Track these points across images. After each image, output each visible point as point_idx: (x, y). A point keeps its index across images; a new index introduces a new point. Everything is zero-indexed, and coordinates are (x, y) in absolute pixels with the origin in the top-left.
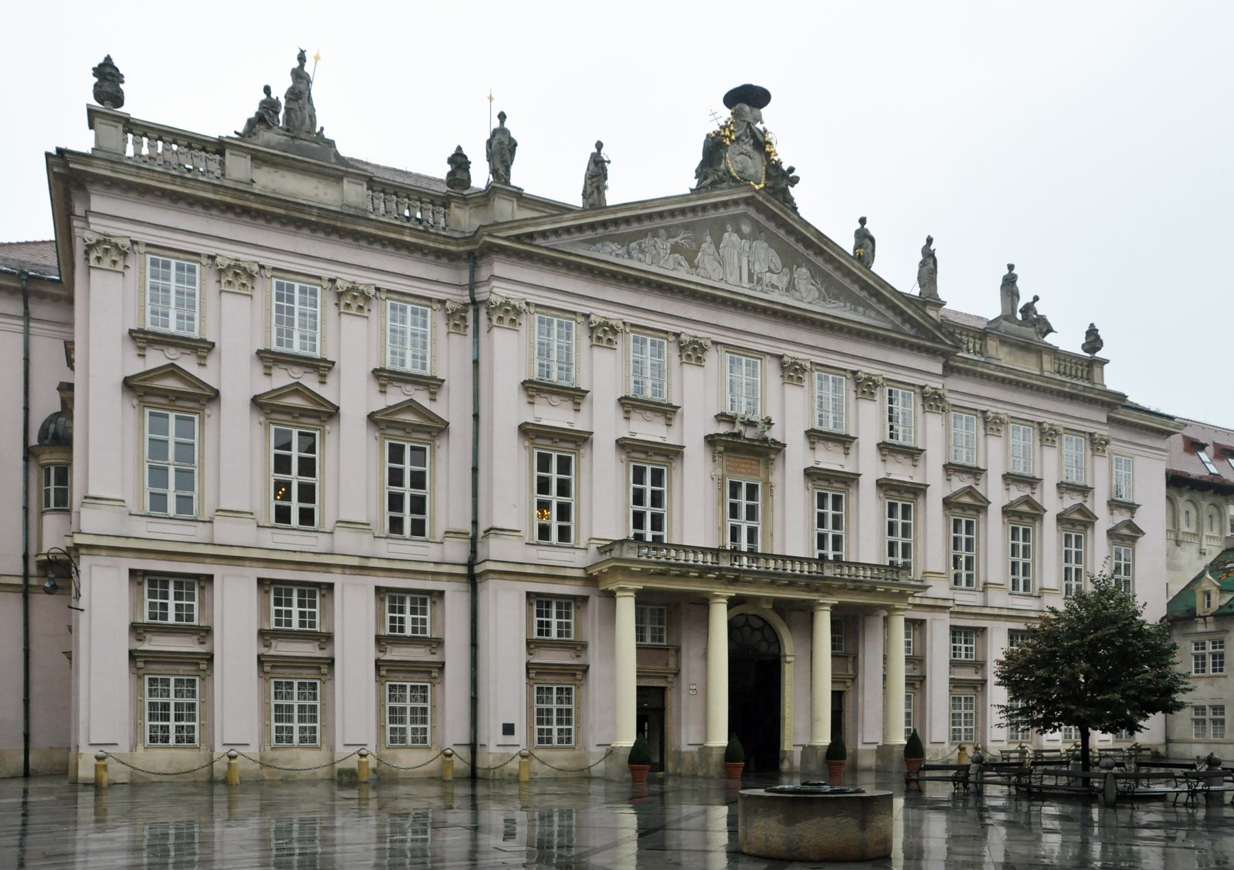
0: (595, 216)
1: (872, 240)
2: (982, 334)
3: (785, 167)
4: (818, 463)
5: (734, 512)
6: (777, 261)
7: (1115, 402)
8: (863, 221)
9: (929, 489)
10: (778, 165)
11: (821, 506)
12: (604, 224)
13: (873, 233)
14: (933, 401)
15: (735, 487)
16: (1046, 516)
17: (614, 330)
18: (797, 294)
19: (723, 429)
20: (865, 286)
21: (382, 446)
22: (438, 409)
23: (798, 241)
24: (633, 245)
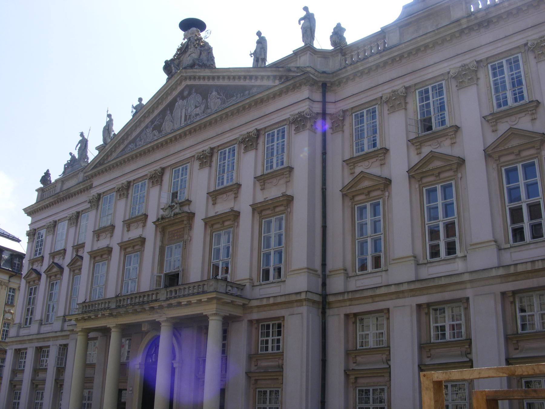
6: (199, 98)
18: (209, 111)
24: (138, 139)
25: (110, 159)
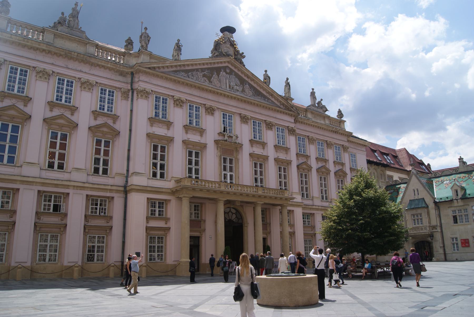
0: (177, 63)
1: (269, 78)
2: (306, 110)
3: (241, 52)
4: (254, 152)
5: (225, 169)
7: (350, 135)
8: (266, 71)
9: (292, 162)
10: (238, 52)
11: (255, 167)
12: (180, 66)
13: (269, 75)
14: (292, 131)
15: (225, 160)
16: (331, 173)
17: (182, 102)
18: (245, 94)
19: (221, 138)
20: (268, 93)
21: (93, 140)
22: (117, 126)
23: (245, 76)
24: (190, 73)
25: (162, 70)
